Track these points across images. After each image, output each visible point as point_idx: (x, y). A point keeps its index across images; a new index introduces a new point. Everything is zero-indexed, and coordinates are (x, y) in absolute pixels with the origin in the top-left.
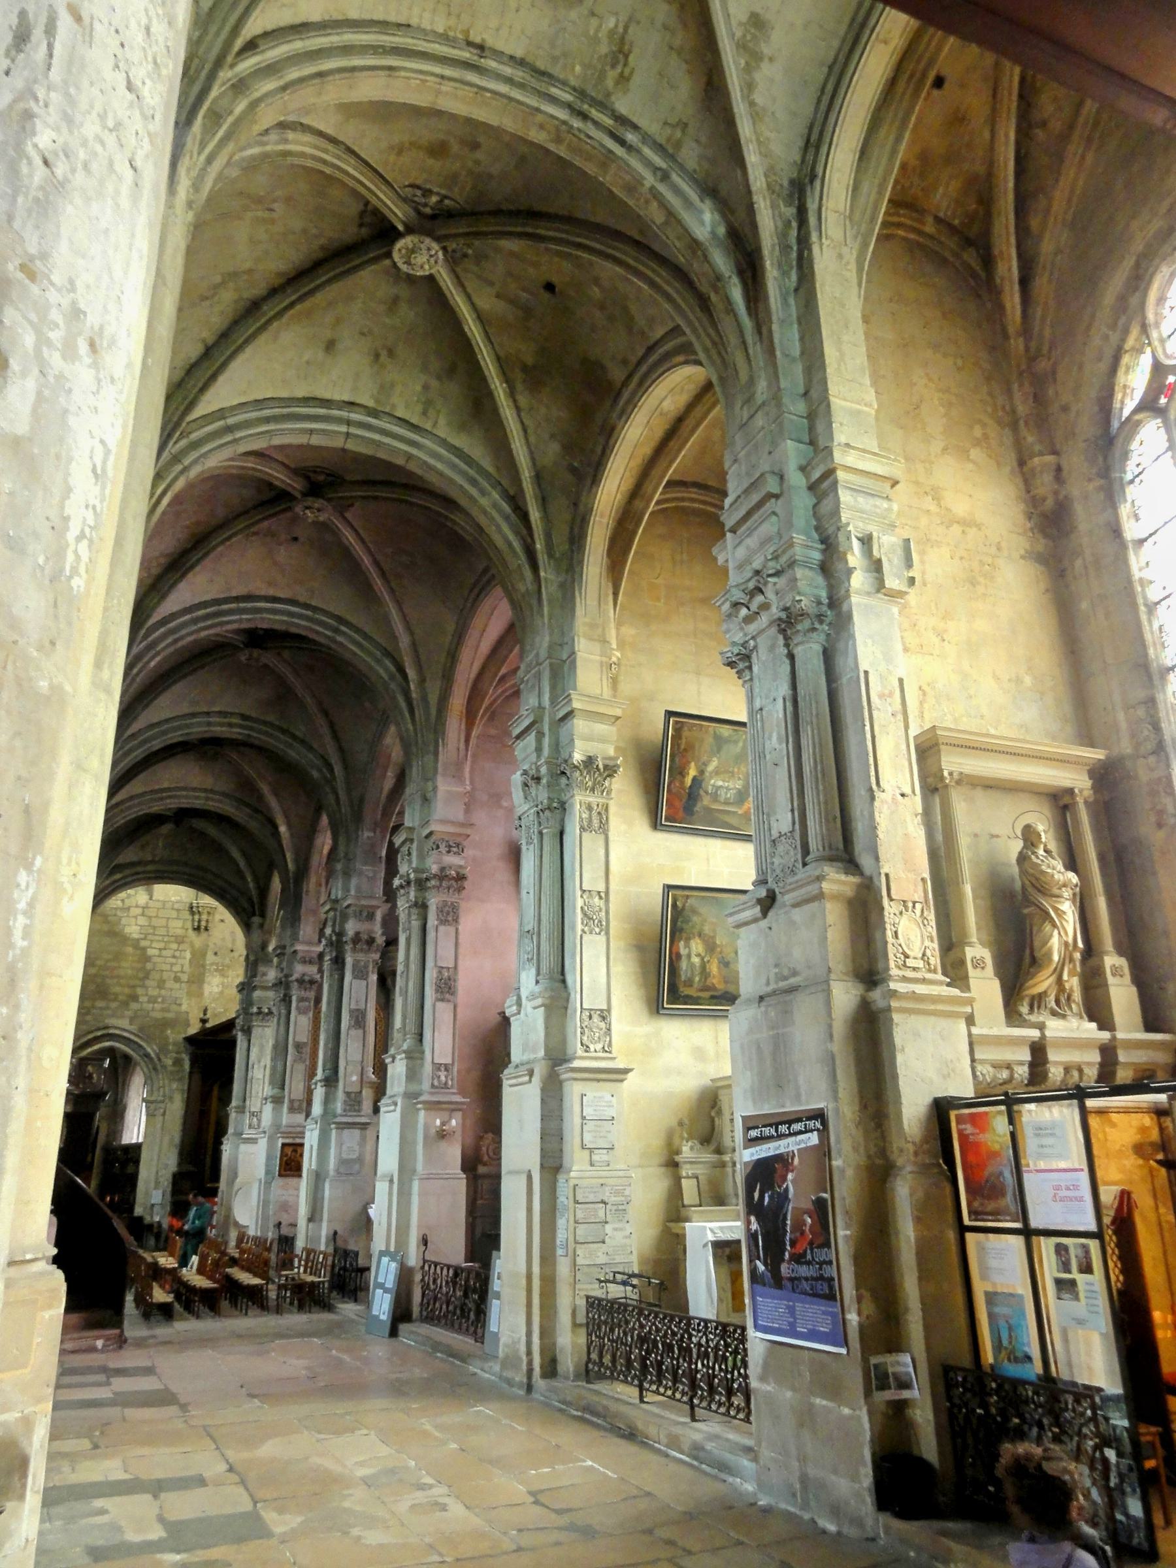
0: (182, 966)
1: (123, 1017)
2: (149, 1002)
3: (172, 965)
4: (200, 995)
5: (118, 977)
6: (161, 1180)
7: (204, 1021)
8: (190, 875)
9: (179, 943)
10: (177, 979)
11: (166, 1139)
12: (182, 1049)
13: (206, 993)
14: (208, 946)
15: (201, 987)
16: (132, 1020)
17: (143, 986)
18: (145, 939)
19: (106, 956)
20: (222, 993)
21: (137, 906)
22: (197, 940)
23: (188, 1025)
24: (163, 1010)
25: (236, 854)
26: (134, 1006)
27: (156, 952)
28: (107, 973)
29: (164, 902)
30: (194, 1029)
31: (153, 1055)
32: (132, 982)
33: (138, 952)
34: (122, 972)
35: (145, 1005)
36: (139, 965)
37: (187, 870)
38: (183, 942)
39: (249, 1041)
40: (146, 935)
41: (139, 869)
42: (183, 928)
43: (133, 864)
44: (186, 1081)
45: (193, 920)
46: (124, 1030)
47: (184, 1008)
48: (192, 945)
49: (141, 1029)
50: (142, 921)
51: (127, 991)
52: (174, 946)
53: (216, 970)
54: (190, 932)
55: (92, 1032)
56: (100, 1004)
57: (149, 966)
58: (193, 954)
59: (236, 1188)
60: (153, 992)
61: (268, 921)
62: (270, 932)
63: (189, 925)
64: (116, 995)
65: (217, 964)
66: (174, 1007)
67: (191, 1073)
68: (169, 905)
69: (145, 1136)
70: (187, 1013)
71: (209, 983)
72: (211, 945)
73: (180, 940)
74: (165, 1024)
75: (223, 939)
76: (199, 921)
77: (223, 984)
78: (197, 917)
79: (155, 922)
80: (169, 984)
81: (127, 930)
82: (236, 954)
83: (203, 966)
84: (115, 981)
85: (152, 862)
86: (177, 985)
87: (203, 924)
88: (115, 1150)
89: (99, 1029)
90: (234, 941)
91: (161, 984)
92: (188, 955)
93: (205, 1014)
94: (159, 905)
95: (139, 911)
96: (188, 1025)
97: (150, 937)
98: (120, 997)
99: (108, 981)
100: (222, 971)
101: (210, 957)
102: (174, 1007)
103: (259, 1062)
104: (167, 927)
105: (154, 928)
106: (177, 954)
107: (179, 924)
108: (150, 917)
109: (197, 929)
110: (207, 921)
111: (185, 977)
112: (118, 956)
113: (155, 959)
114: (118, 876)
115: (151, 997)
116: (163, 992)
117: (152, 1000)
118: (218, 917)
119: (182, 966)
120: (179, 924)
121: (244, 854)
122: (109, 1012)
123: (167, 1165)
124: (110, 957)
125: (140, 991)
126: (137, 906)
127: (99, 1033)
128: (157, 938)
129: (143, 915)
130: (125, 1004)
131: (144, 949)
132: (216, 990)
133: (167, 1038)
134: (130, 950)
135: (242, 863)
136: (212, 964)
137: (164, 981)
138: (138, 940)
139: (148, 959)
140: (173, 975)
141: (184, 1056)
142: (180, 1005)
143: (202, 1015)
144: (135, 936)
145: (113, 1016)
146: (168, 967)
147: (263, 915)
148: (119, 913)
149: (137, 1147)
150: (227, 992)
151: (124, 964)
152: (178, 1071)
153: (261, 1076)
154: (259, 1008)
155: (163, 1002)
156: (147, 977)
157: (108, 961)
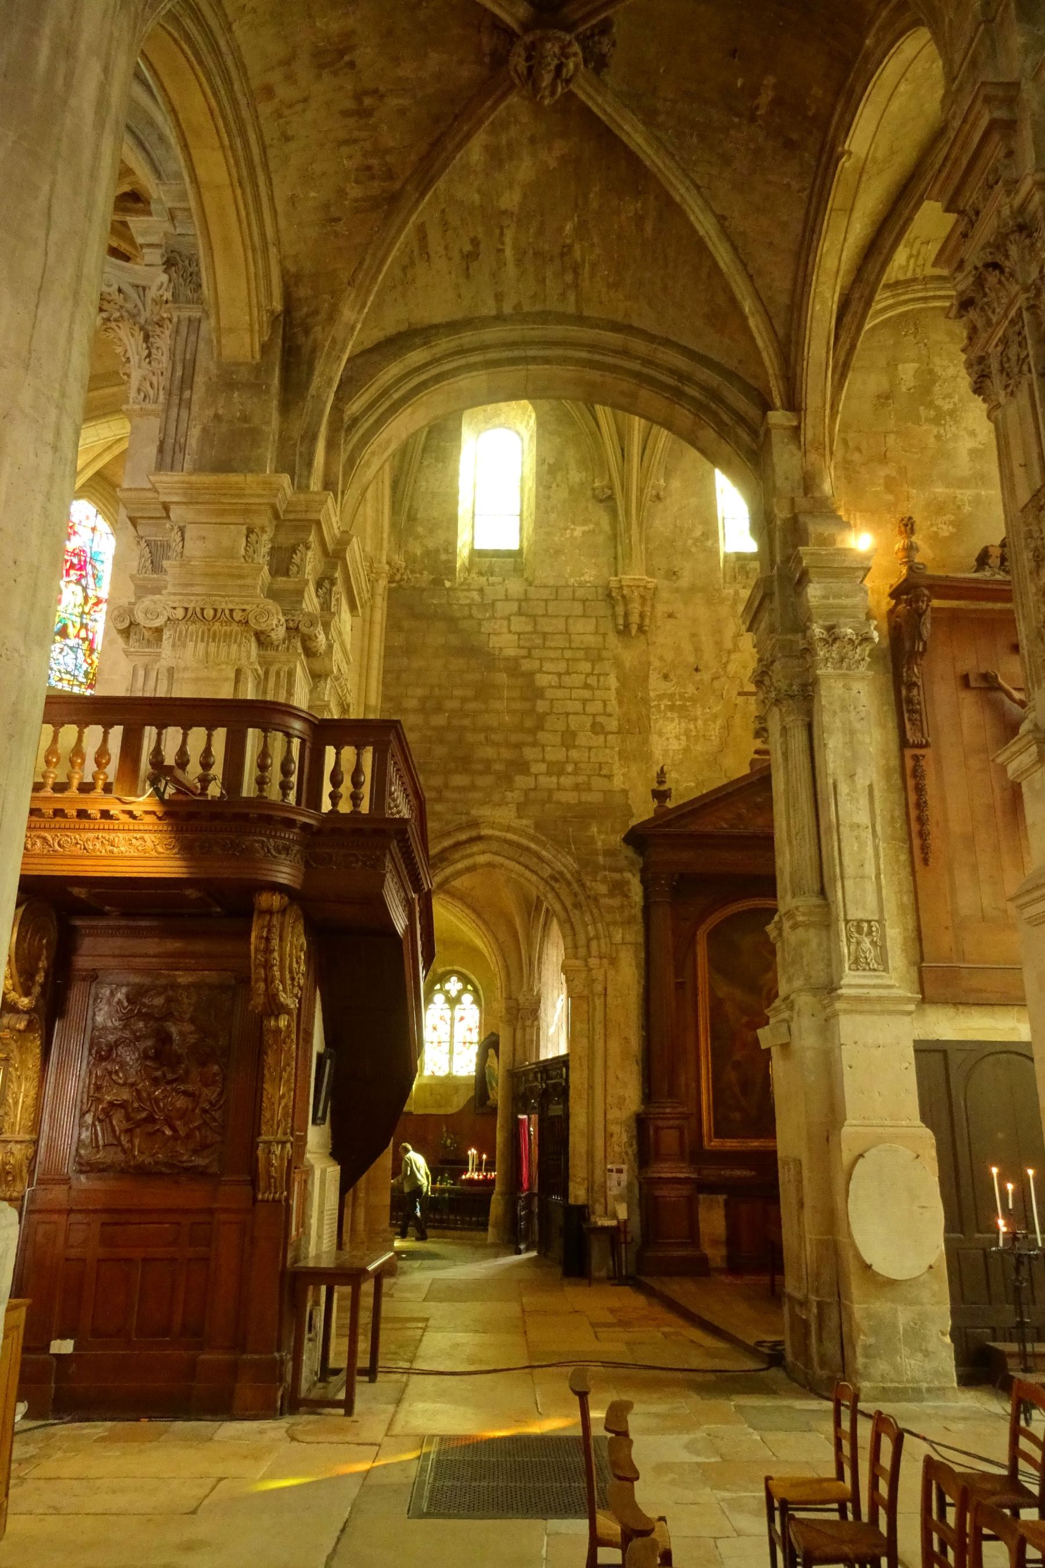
0: (605, 703)
1: (502, 803)
2: (549, 774)
3: (585, 701)
4: (647, 757)
5: (488, 729)
6: (615, 1129)
7: (661, 795)
8: (592, 347)
9: (593, 663)
10: (597, 729)
11: (615, 1046)
12: (623, 863)
13: (657, 753)
14: (649, 663)
15: (646, 742)
16: (521, 809)
17: (534, 744)
18: (529, 656)
19: (457, 692)
20: (687, 750)
21: (507, 599)
22: (629, 657)
23: (632, 815)
24: (576, 787)
25: (705, 225)
26: (521, 781)
27: (554, 680)
28: (467, 722)
29: (557, 589)
30: (644, 810)
31: (568, 876)
32: (514, 738)
33: (520, 681)
34: (492, 721)
35: (546, 781)
36: (527, 705)
37: (587, 334)
38: (600, 659)
39: (809, 727)
40: (529, 649)
41: (468, 338)
42: (596, 633)
43: (453, 327)
44: (639, 927)
45: (614, 616)
46: (509, 829)
47: (618, 782)
48: (618, 663)
49: (538, 826)
50: (519, 624)
51: (506, 754)
52: (586, 667)
53: (672, 708)
54: (612, 639)
55: (448, 834)
56: (459, 780)
57: (541, 706)
58: (623, 680)
59: (846, 1157)
60: (555, 755)
61: (810, 419)
62: (819, 447)
63: (607, 626)
64: (488, 763)
65: (671, 697)
66: (597, 783)
67: (646, 910)
68: (567, 594)
69: (572, 1040)
70: (625, 792)
71: (660, 734)
72: (656, 663)
73: (595, 656)
74: (585, 815)
75: (678, 649)
76: (626, 615)
77: (687, 733)
78: (620, 610)
79: (546, 626)
80: (583, 739)
81: (494, 642)
82: (706, 676)
83: (645, 701)
84: (482, 737)
85: (499, 318)
86: (602, 738)
87: (635, 619)
88: (525, 1073)
89: (460, 829)
90: (697, 650)
91: (569, 739)
92: (613, 682)
93: (661, 783)
94: (545, 593)
95: (514, 607)
96: (632, 815)
97: (536, 653)
98: (497, 767)
99: (470, 737)
100: (681, 709)
101: (656, 685)
102: (597, 783)
103: (852, 776)
104: (567, 632)
105: (545, 636)
106: (592, 681)
107: (590, 626)
108: (534, 618)
109: (624, 632)
110: (642, 616)
111: (613, 725)
112: (484, 691)
113: (549, 694)
114: (417, 357)
115: (550, 764)
116: (574, 754)
117: (557, 769)
118: (661, 609)
119: (605, 703)
120: (590, 626)
121: (725, 232)
122: (477, 795)
123: (622, 1101)
124: (470, 693)
125: (529, 753)
126: (507, 599)
127: (463, 837)
128: (552, 654)
129: (520, 613)
130: (506, 780)
131: (530, 675)
132: (675, 745)
133: (592, 840)
134: (502, 678)
135: (723, 255)
136: (660, 697)
137: (574, 734)
138: (516, 659)
139: (539, 693)
140: (588, 722)
141: (628, 875)
142: (609, 777)
143: (655, 786)
144: (511, 652)
145: (483, 803)
146: (578, 706)
147: (794, 404)
148: (475, 612)
149: (562, 1062)
150: (699, 748)
151: (497, 705)
152: (622, 907)
153: (864, 818)
154: (830, 629)
155: (576, 773)
156: (540, 727)
157: (464, 700)
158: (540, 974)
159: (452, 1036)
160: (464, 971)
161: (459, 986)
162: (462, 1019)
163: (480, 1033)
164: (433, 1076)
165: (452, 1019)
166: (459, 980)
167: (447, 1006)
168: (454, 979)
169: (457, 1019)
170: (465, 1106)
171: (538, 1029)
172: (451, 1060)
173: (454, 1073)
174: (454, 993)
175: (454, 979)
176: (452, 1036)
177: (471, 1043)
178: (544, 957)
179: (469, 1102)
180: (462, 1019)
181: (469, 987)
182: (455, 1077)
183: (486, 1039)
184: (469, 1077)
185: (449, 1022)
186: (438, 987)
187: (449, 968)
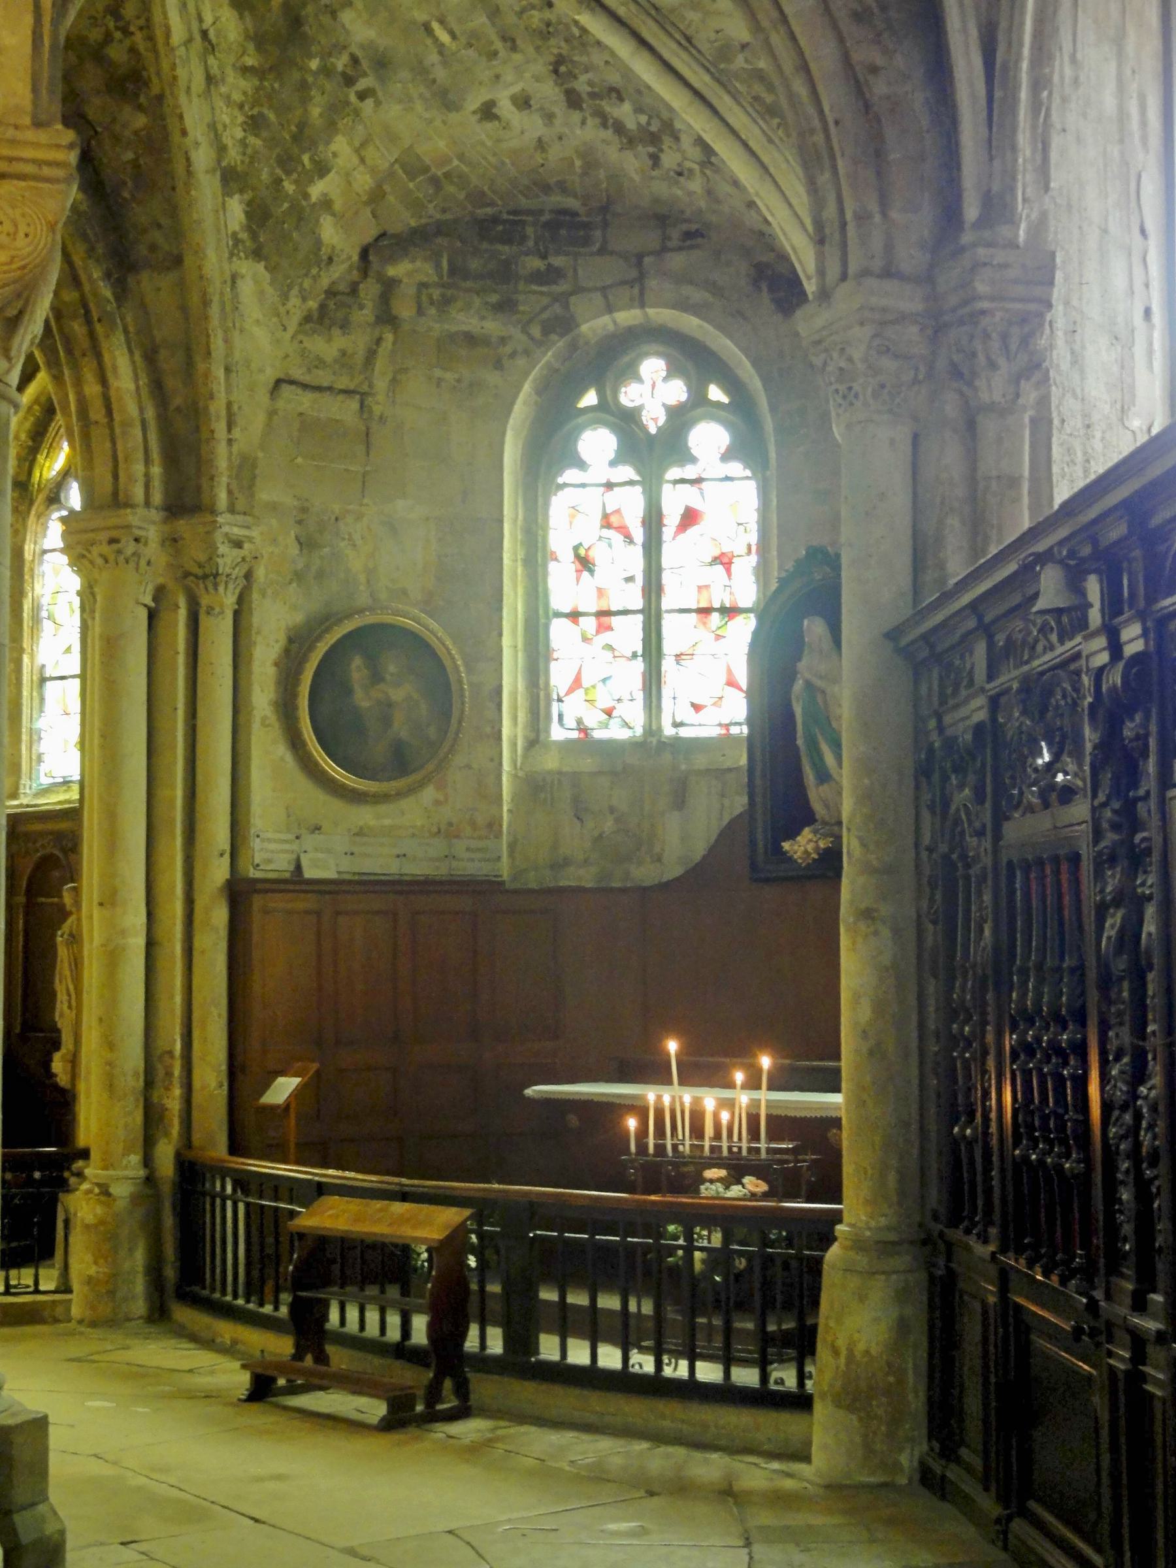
158: (1043, 146)
159: (653, 587)
160: (691, 323)
161: (677, 391)
162: (690, 518)
163: (762, 572)
164: (585, 744)
165: (653, 521)
166: (673, 371)
167: (627, 472)
168: (653, 367)
169: (672, 517)
170: (712, 851)
171: (1042, 426)
172: (653, 682)
173: (668, 731)
174: (654, 418)
175: (653, 367)
176: (653, 587)
177: (729, 612)
178: (1062, 70)
179: (727, 833)
180: (690, 518)
181: (715, 393)
182: (677, 744)
183: (783, 582)
184: (727, 740)
185: (638, 534)
186: (590, 398)
187: (627, 317)
